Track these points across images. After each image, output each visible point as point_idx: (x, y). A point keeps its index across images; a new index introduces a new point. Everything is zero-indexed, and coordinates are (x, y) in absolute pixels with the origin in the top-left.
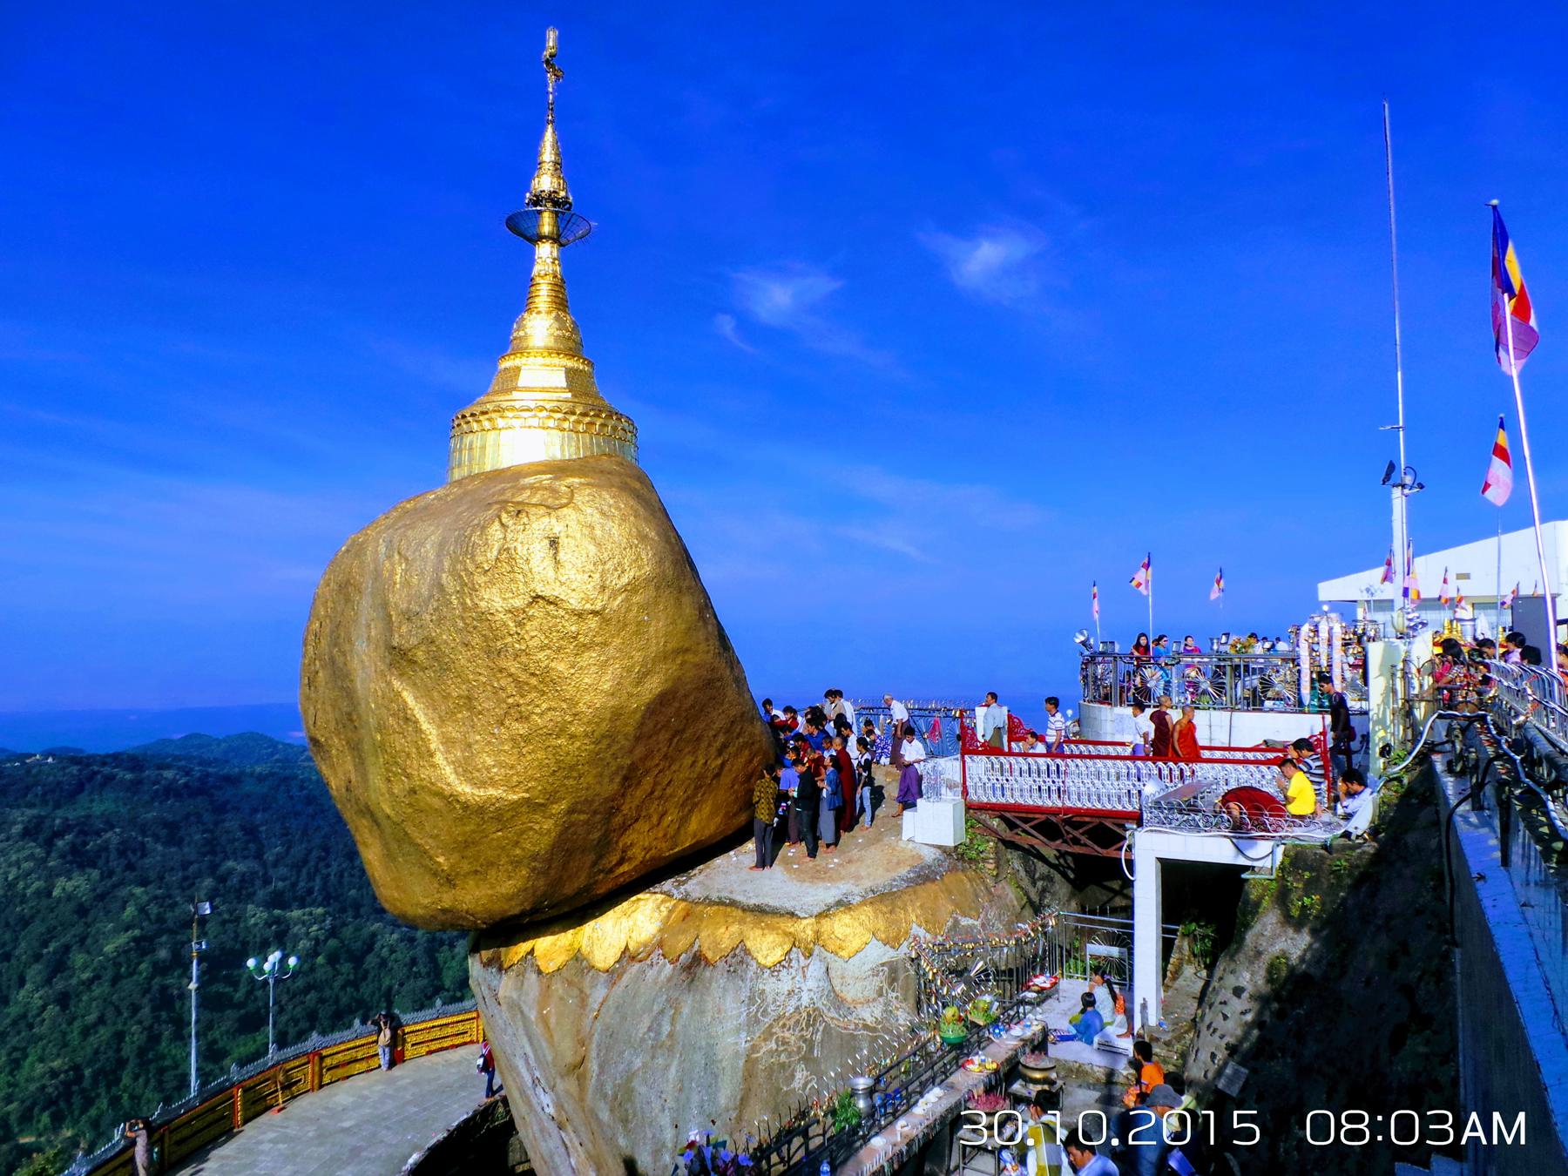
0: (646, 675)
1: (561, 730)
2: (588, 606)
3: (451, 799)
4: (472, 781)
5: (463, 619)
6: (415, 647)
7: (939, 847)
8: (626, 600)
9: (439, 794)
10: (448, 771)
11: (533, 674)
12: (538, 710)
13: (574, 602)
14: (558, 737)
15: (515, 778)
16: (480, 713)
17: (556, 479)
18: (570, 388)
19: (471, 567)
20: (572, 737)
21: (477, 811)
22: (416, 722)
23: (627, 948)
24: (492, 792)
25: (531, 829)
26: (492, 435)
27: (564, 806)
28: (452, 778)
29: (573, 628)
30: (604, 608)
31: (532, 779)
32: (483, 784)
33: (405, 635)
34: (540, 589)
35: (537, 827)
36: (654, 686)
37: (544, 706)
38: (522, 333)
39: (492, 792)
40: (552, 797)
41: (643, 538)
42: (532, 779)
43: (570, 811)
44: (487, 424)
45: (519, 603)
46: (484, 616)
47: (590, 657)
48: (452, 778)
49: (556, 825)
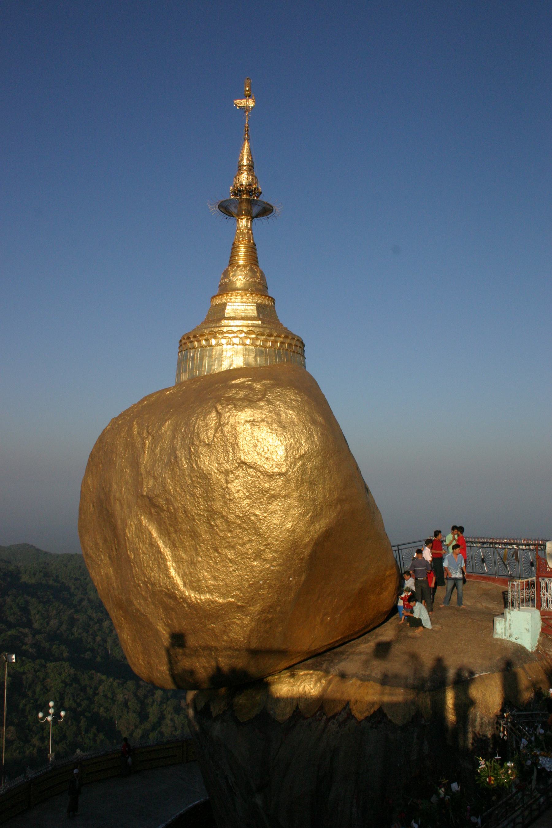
2: (276, 470)
4: (194, 589)
5: (190, 476)
8: (303, 465)
12: (240, 541)
13: (268, 467)
14: (255, 560)
17: (254, 381)
20: (265, 560)
23: (297, 707)
25: (234, 623)
29: (267, 485)
30: (287, 471)
36: (321, 526)
37: (246, 539)
40: (251, 601)
41: (314, 422)
43: (262, 611)
46: (205, 477)
47: (276, 506)
49: (252, 620)
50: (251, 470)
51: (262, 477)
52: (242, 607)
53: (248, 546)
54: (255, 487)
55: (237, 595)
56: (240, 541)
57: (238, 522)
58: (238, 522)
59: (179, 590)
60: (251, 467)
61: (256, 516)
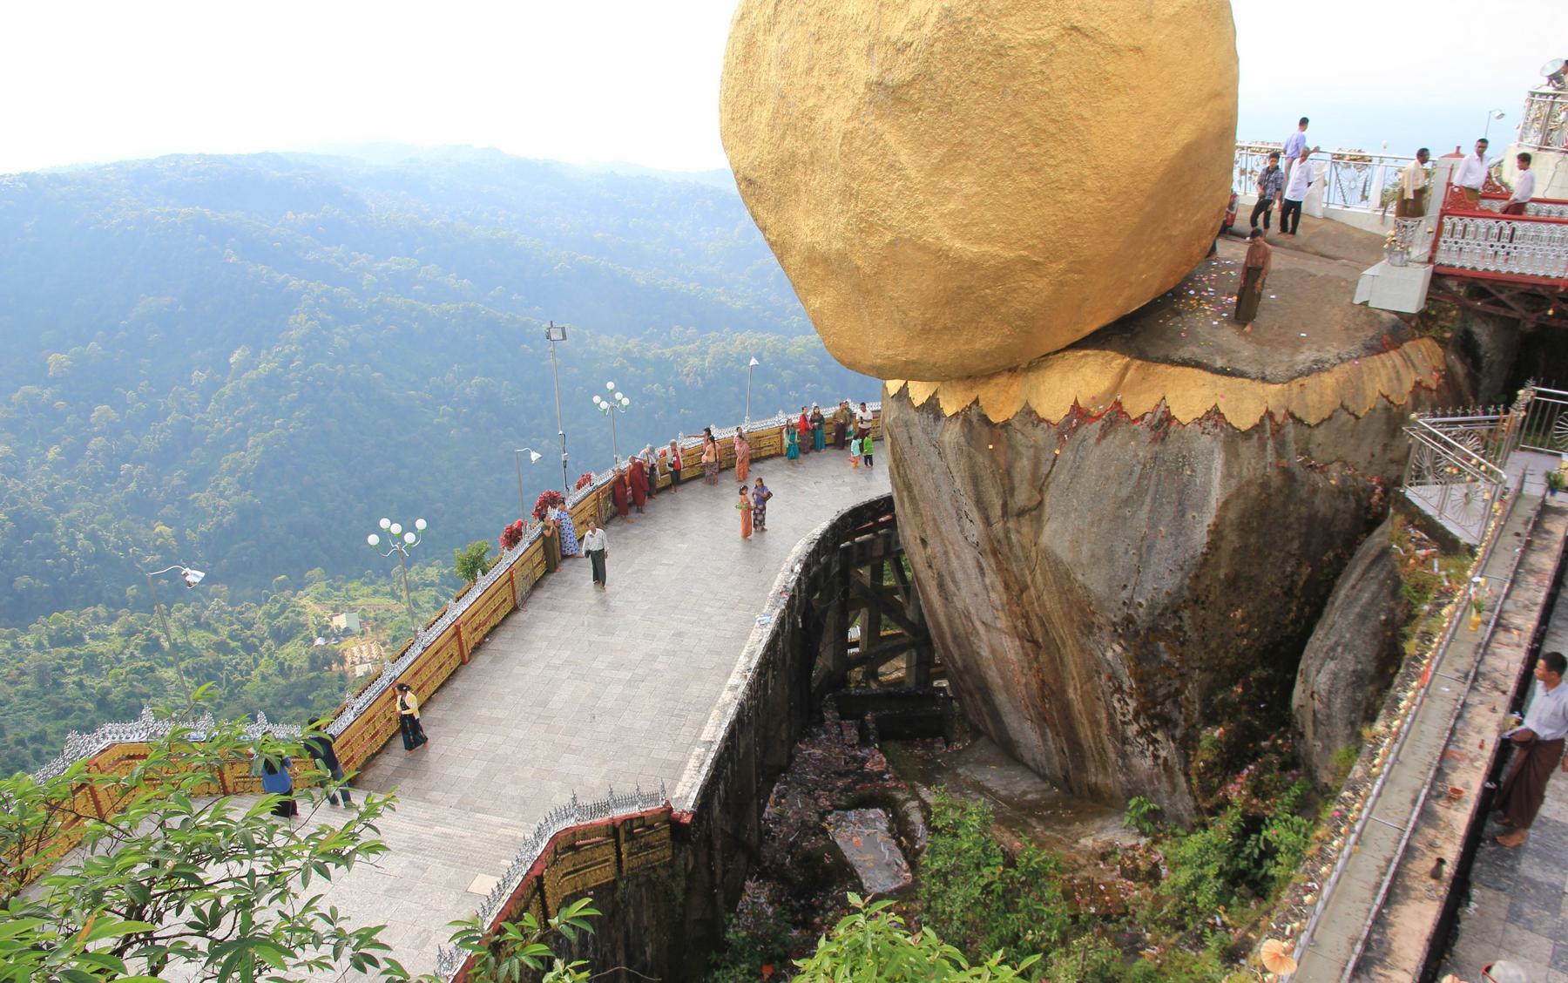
1: (1078, 184)
2: (1129, 41)
3: (941, 254)
4: (961, 236)
6: (910, 84)
7: (1397, 313)
9: (924, 248)
11: (1053, 121)
12: (1052, 162)
14: (1071, 191)
15: (1015, 235)
16: (983, 162)
21: (973, 266)
24: (986, 248)
25: (1021, 287)
27: (1063, 265)
31: (1033, 236)
32: (978, 240)
34: (1077, 18)
35: (1029, 286)
37: (1061, 157)
39: (986, 248)
42: (1033, 236)
45: (1047, 35)
46: (1000, 52)
51: (1103, 53)
52: (1037, 263)
53: (1064, 169)
54: (1089, 71)
55: (1033, 247)
56: (1052, 162)
57: (1052, 128)
58: (1052, 128)
61: (1083, 119)
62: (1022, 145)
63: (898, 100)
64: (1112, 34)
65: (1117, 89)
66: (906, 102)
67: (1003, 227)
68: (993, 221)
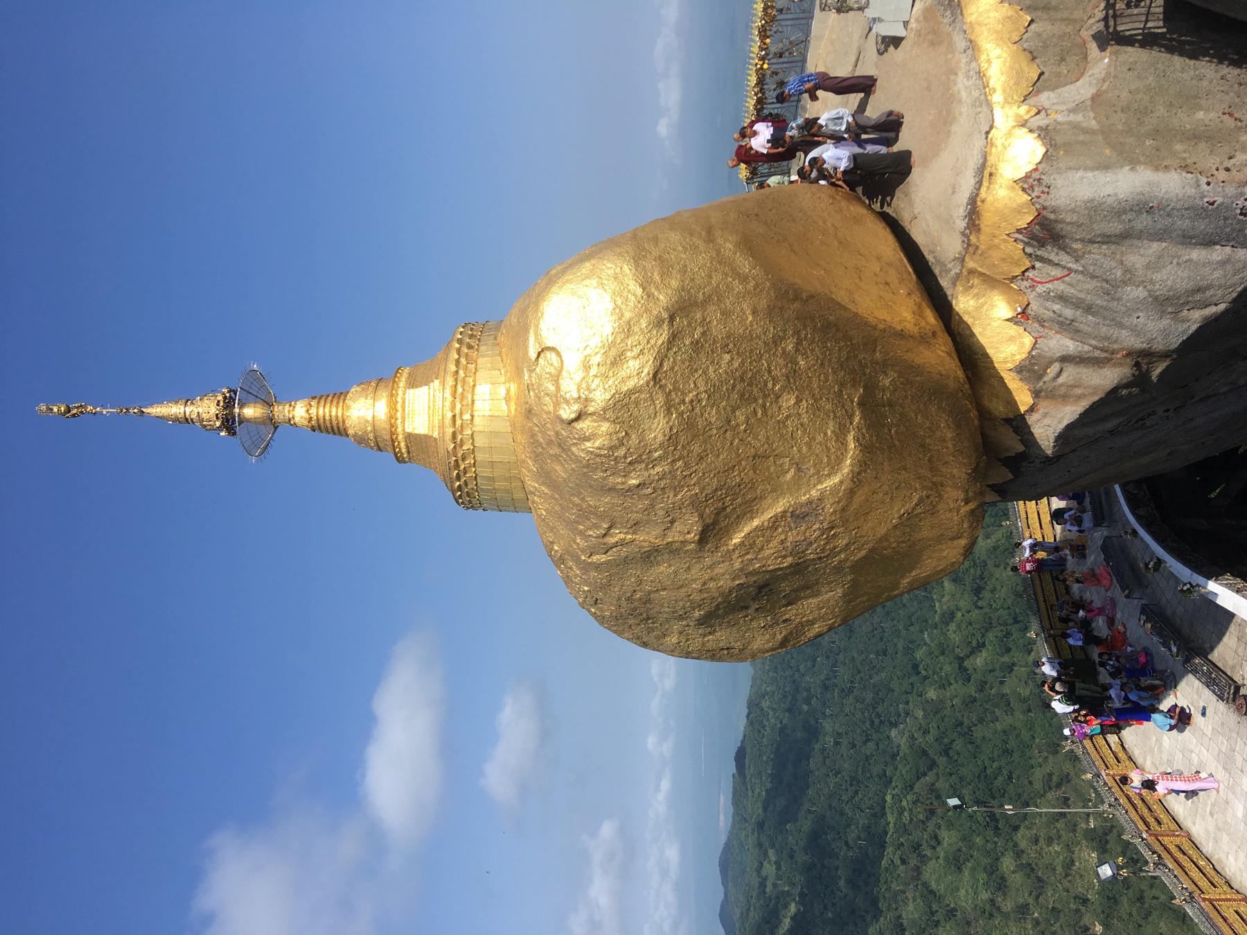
0: (733, 270)
2: (665, 326)
4: (839, 460)
6: (701, 516)
9: (851, 493)
10: (829, 483)
12: (770, 385)
18: (427, 382)
19: (622, 452)
20: (797, 350)
22: (776, 516)
26: (480, 456)
28: (836, 479)
32: (844, 444)
33: (688, 528)
38: (371, 436)
39: (850, 437)
44: (470, 461)
46: (672, 439)
48: (836, 479)
50: (665, 364)
59: (841, 482)
60: (661, 364)
62: (755, 413)
63: (715, 523)
64: (660, 342)
65: (704, 334)
66: (717, 514)
67: (831, 424)
68: (825, 434)
